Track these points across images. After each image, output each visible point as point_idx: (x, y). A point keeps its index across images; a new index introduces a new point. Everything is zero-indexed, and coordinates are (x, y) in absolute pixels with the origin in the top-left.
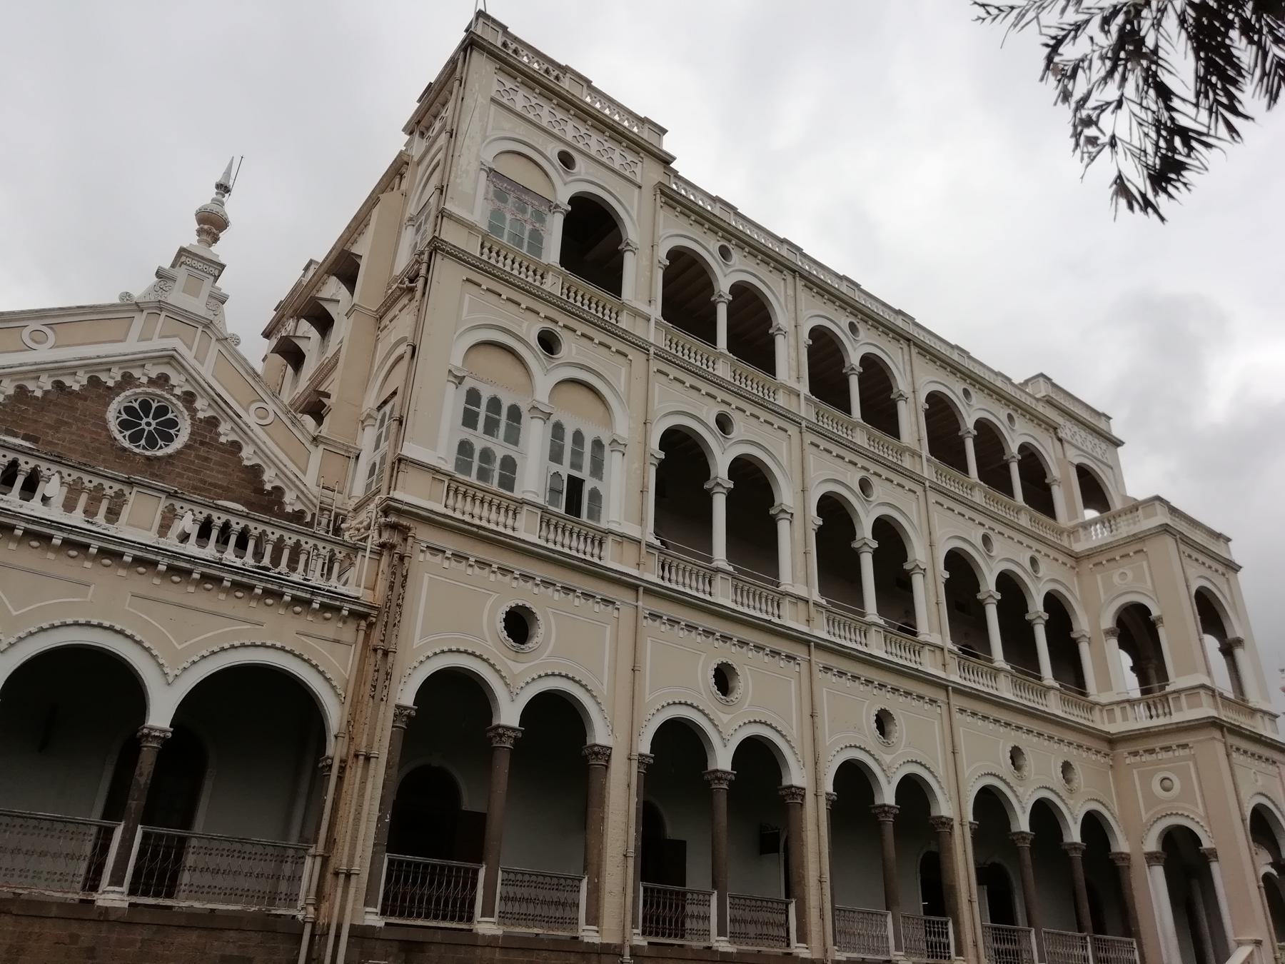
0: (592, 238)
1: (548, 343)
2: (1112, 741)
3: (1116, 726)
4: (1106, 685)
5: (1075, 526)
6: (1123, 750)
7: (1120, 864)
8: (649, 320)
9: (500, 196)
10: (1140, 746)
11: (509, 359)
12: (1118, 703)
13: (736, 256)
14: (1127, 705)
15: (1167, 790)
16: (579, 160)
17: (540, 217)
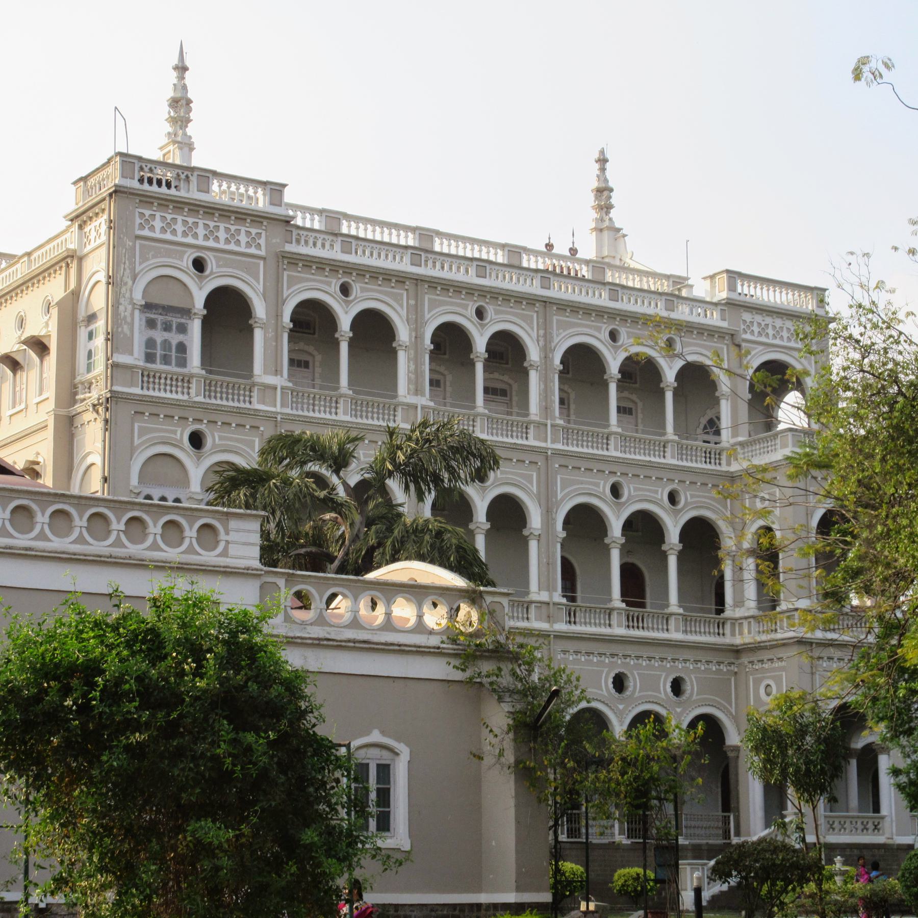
0: (228, 313)
1: (196, 440)
2: (737, 651)
3: (738, 641)
4: (739, 602)
5: (735, 444)
6: (745, 660)
7: (731, 755)
8: (276, 388)
9: (151, 324)
10: (766, 655)
11: (169, 459)
12: (746, 618)
13: (356, 288)
14: (752, 620)
15: (768, 694)
16: (211, 265)
17: (182, 329)
